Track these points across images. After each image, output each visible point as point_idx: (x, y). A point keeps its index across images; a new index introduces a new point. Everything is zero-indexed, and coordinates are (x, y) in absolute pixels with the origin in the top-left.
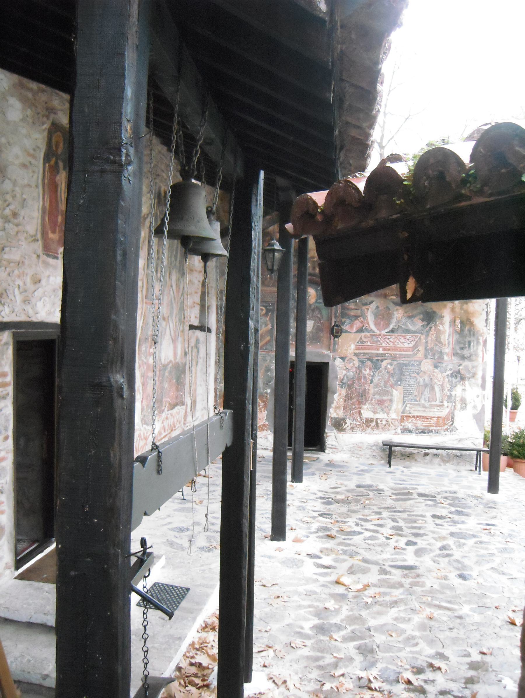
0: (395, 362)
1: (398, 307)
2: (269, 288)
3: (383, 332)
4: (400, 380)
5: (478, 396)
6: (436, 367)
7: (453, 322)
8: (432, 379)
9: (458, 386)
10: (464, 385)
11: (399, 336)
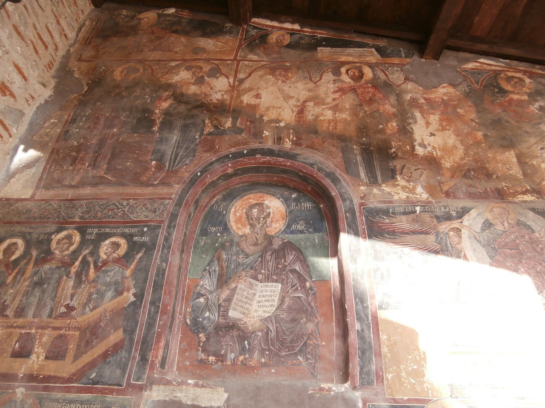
2: (149, 190)
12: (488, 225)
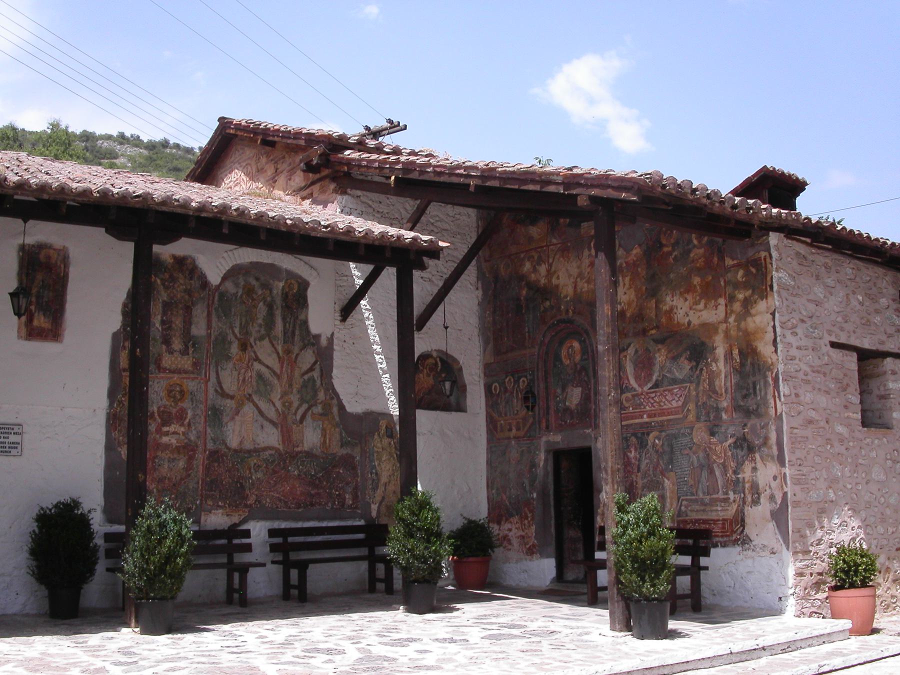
0: (663, 434)
1: (660, 346)
3: (646, 389)
4: (671, 461)
5: (775, 478)
6: (712, 434)
7: (729, 355)
8: (708, 455)
9: (746, 462)
10: (754, 460)
11: (664, 391)
12: (636, 351)
